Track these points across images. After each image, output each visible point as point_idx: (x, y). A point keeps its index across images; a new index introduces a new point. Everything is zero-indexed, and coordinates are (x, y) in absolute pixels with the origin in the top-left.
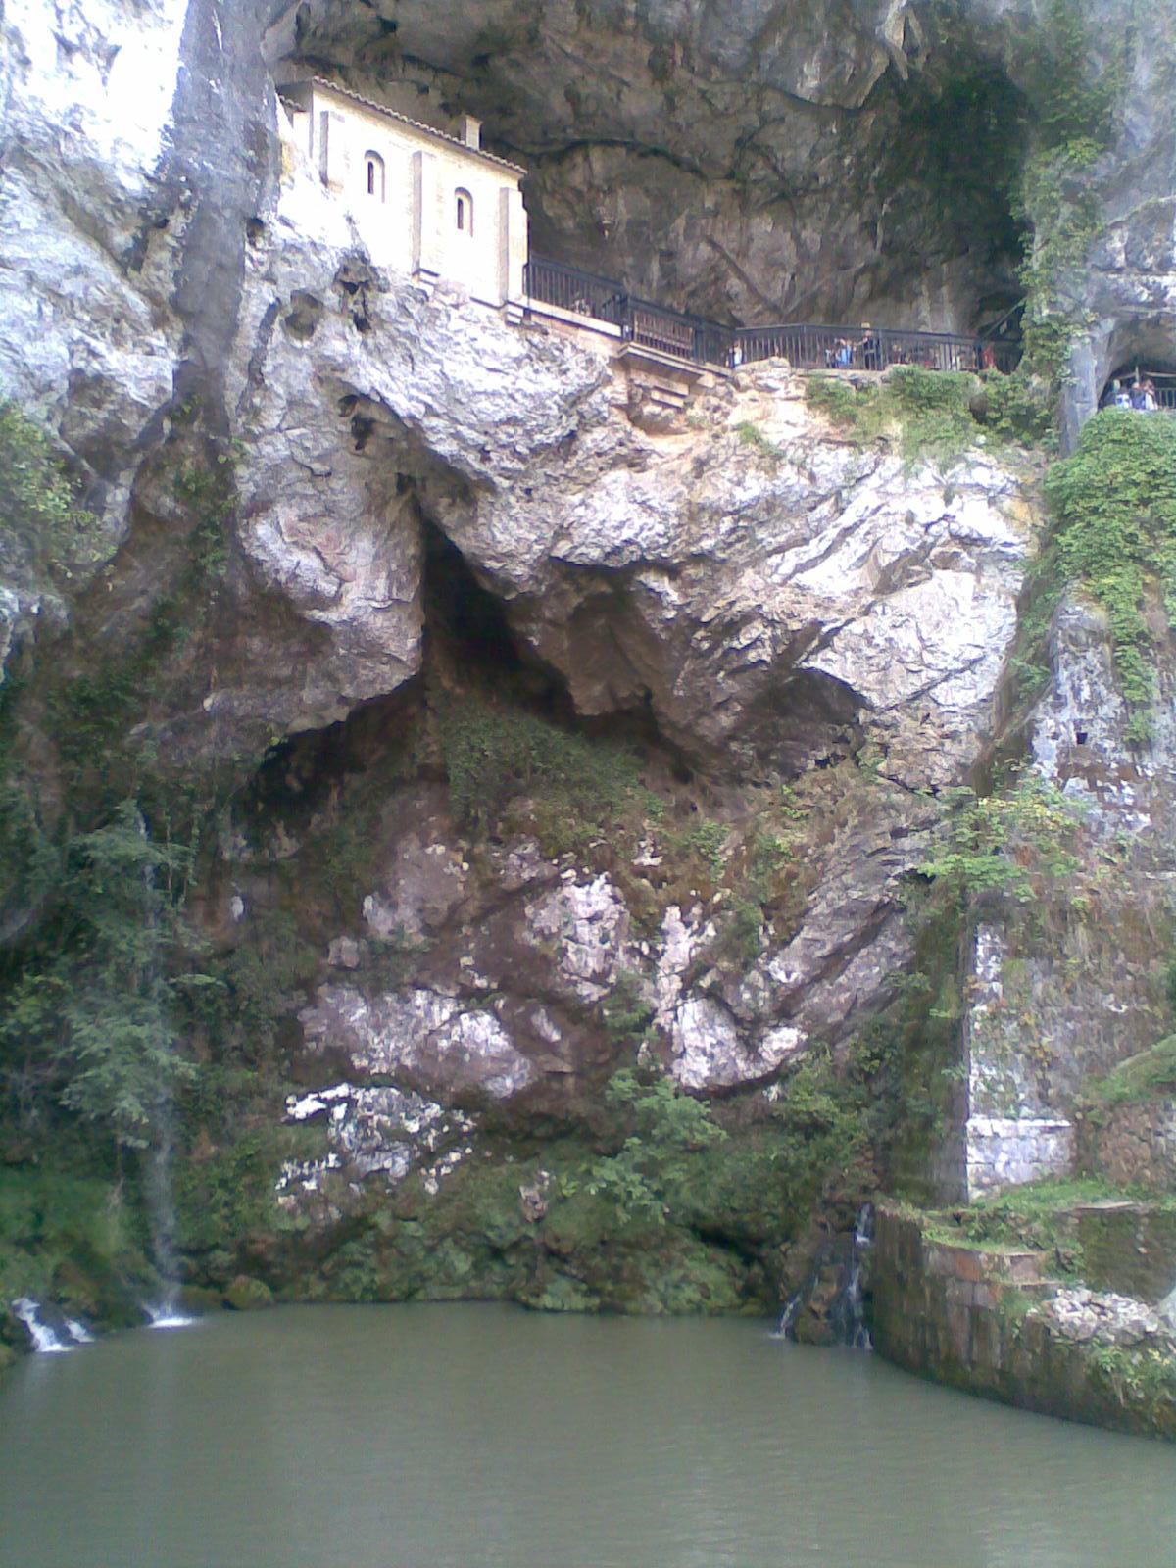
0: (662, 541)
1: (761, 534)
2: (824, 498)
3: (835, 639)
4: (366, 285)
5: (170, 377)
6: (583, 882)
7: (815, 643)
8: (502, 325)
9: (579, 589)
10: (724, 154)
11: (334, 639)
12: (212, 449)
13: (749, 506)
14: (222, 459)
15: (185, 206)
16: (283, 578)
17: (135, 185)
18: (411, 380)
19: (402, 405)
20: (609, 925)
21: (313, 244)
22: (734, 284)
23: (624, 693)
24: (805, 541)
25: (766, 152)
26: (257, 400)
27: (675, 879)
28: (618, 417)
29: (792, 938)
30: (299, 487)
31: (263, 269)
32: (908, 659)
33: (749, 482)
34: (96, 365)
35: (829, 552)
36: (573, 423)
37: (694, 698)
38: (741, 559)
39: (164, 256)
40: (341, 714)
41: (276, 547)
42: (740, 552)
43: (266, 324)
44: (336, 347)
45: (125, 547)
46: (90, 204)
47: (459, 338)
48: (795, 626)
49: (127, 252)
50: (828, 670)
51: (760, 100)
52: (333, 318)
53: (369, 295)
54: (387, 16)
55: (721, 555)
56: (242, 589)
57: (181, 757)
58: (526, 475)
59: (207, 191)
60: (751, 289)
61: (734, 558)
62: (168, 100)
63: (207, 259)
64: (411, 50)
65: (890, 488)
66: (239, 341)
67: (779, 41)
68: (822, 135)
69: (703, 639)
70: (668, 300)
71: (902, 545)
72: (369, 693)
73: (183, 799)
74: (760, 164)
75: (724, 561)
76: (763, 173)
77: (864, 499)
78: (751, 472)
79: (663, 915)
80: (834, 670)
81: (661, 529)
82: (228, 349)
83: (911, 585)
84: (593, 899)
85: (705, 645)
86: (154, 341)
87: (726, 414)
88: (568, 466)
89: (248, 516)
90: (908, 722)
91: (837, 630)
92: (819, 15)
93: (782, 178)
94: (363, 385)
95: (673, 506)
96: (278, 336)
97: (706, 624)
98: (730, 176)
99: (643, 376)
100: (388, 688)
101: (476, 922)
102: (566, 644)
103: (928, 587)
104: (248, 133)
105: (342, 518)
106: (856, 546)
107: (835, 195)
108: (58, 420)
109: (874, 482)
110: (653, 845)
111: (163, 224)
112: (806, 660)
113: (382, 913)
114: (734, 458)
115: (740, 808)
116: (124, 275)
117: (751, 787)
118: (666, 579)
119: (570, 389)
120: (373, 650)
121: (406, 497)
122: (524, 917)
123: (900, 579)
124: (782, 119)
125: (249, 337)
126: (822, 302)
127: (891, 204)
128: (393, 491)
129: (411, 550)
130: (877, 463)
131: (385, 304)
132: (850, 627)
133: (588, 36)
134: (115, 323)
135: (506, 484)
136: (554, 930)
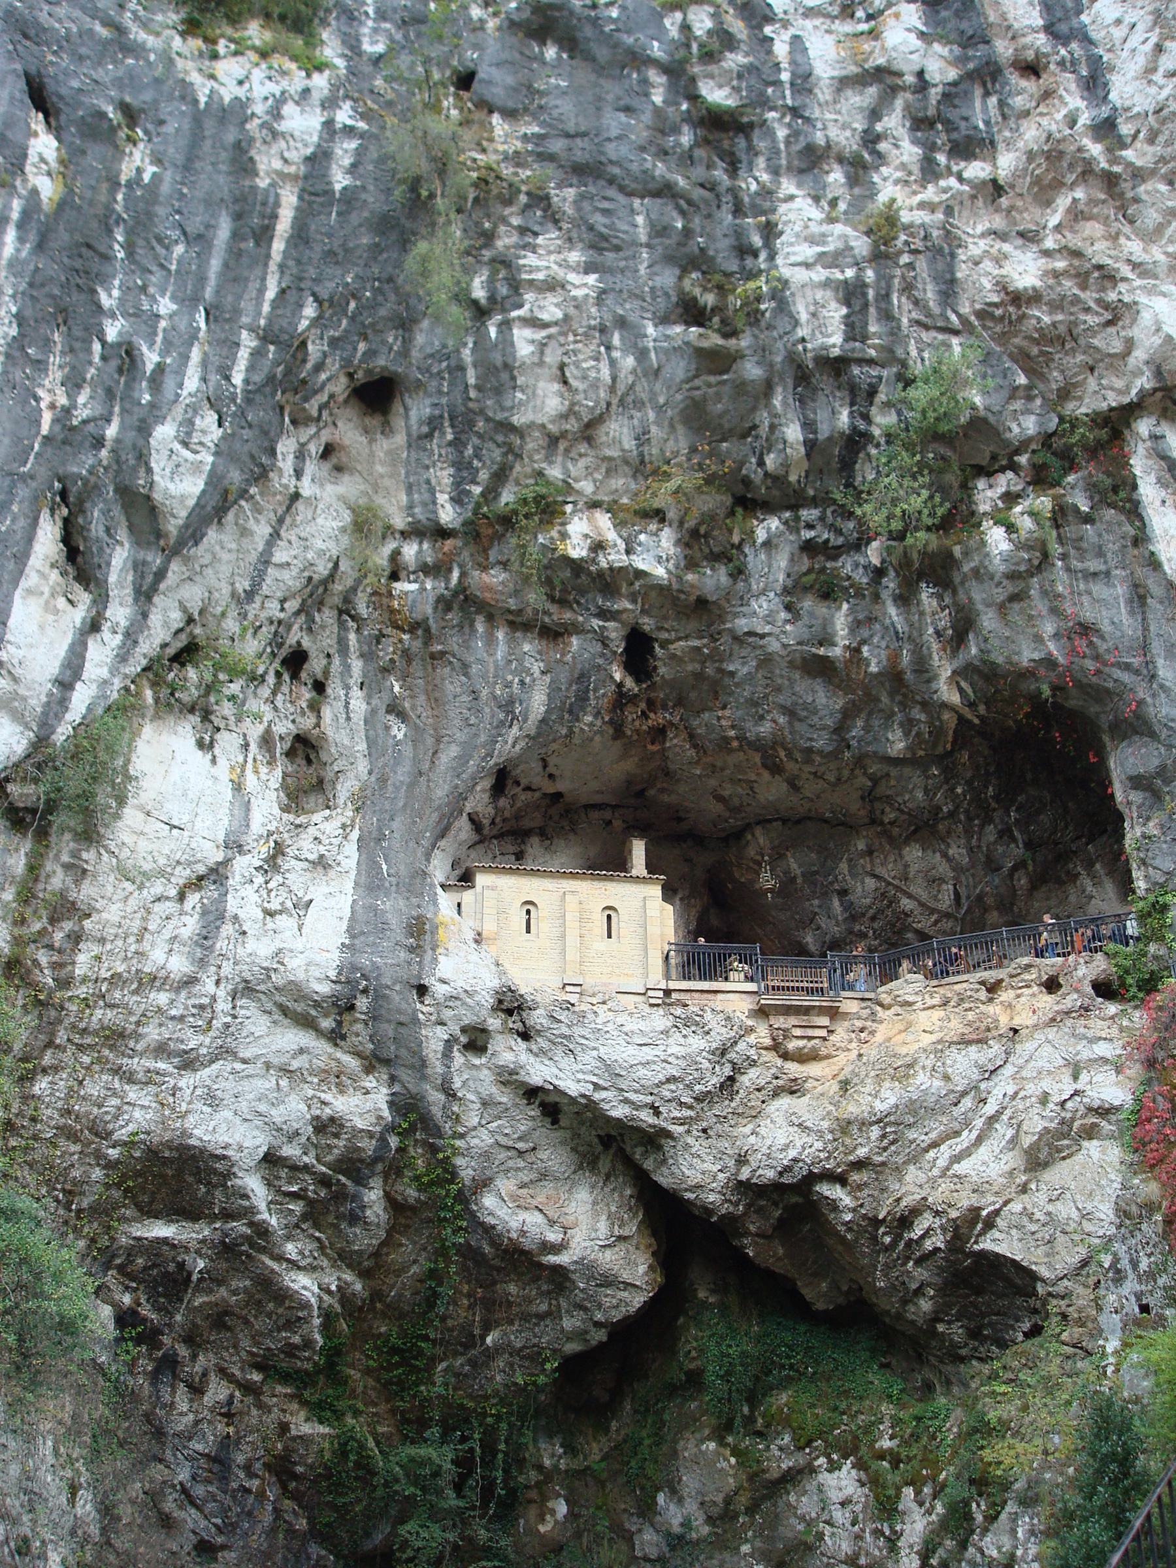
0: (822, 1155)
1: (912, 1134)
2: (964, 1094)
3: (998, 1220)
4: (520, 1008)
5: (385, 1106)
6: (833, 1467)
7: (980, 1226)
8: (647, 1009)
9: (776, 1204)
10: (855, 806)
11: (573, 1277)
12: (434, 1149)
13: (889, 1114)
14: (441, 1156)
15: (365, 991)
16: (514, 1235)
17: (324, 989)
18: (575, 1067)
19: (572, 1088)
20: (858, 1508)
21: (466, 991)
22: (906, 904)
23: (845, 1288)
24: (957, 1134)
25: (889, 799)
26: (455, 1109)
27: (909, 1459)
28: (770, 1057)
29: (999, 1513)
30: (510, 1163)
31: (433, 1018)
32: (1069, 1229)
33: (885, 1093)
34: (328, 1111)
35: (979, 1140)
36: (727, 1071)
37: (894, 1287)
38: (900, 1159)
39: (359, 1027)
40: (601, 1336)
41: (503, 1212)
42: (897, 1153)
43: (447, 1055)
44: (506, 1058)
45: (390, 1232)
46: (299, 1007)
47: (610, 1026)
48: (954, 1214)
49: (333, 1031)
50: (997, 1249)
51: (864, 767)
52: (499, 1037)
53: (524, 1014)
54: (551, 790)
55: (878, 1159)
56: (487, 1249)
57: (482, 1387)
58: (698, 1118)
59: (376, 979)
60: (922, 904)
61: (893, 1159)
62: (344, 925)
63: (389, 1021)
64: (584, 801)
65: (1024, 1074)
66: (429, 1071)
67: (860, 723)
68: (927, 777)
69: (884, 1234)
70: (857, 928)
71: (1039, 1125)
72: (616, 1316)
73: (489, 1420)
74: (888, 809)
75: (883, 1164)
76: (892, 816)
77: (1001, 1087)
78: (887, 1084)
79: (898, 1496)
80: (1001, 1249)
81: (819, 1145)
82: (424, 1078)
83: (1064, 1158)
84: (844, 1483)
85: (887, 1240)
86: (367, 1085)
87: (873, 1033)
88: (733, 1104)
89: (475, 1193)
90: (1080, 1290)
91: (997, 1212)
92: (885, 699)
93: (909, 814)
94: (536, 1080)
95: (825, 1124)
96: (458, 1059)
97: (884, 1220)
98: (873, 821)
99: (782, 1019)
100: (632, 1310)
101: (751, 1510)
102: (781, 1251)
103: (1079, 1157)
104: (410, 926)
105: (557, 1179)
106: (1003, 1131)
107: (962, 817)
108: (312, 1153)
109: (1009, 1070)
110: (892, 1427)
111: (352, 1008)
112: (976, 1242)
113: (672, 1507)
114: (873, 1074)
115: (966, 1386)
116: (336, 1045)
117: (974, 1362)
118: (838, 1187)
119: (714, 1045)
120: (609, 1281)
121: (612, 1151)
122: (789, 1505)
123: (1050, 1154)
124: (888, 775)
125: (437, 1067)
126: (989, 901)
127: (1017, 811)
128: (600, 1148)
129: (628, 1192)
130: (1008, 1053)
131: (537, 1018)
132: (1010, 1206)
133: (709, 759)
134: (338, 1079)
135: (680, 1129)
136: (814, 1515)
